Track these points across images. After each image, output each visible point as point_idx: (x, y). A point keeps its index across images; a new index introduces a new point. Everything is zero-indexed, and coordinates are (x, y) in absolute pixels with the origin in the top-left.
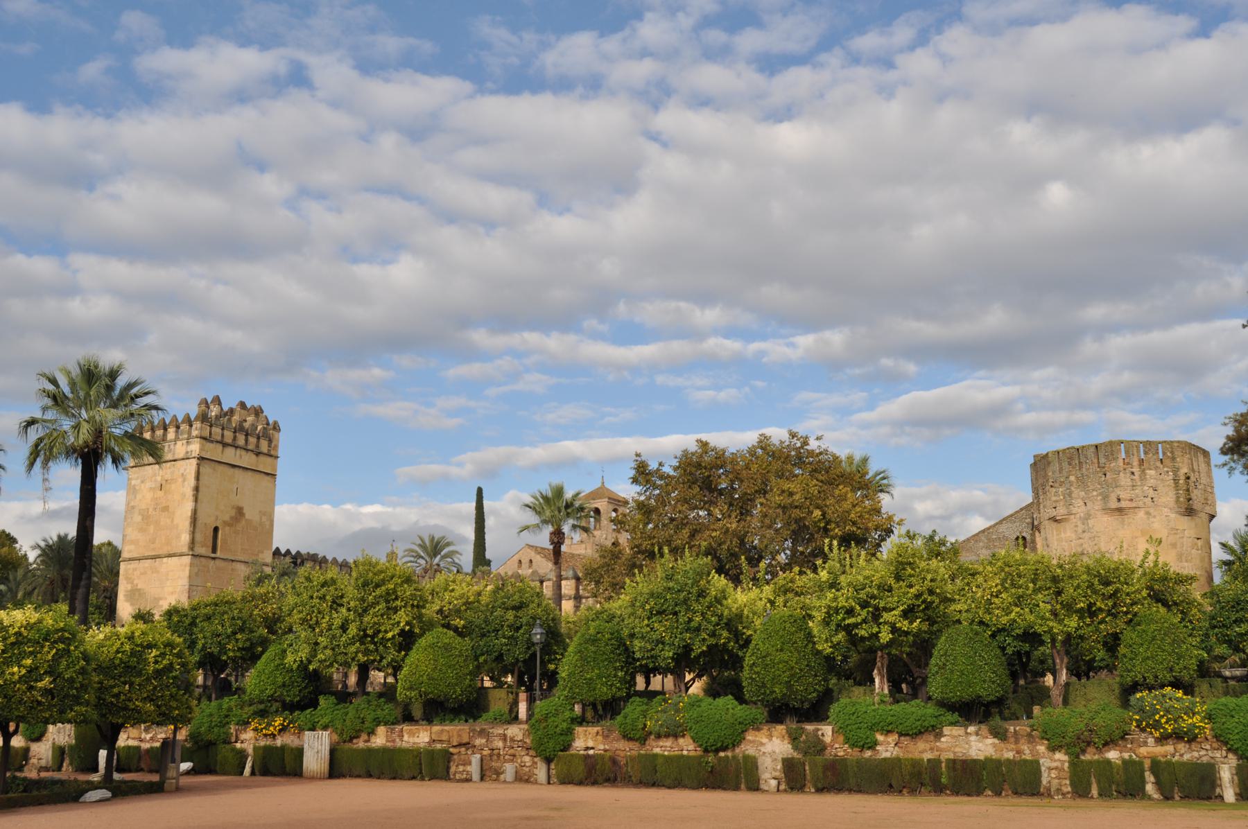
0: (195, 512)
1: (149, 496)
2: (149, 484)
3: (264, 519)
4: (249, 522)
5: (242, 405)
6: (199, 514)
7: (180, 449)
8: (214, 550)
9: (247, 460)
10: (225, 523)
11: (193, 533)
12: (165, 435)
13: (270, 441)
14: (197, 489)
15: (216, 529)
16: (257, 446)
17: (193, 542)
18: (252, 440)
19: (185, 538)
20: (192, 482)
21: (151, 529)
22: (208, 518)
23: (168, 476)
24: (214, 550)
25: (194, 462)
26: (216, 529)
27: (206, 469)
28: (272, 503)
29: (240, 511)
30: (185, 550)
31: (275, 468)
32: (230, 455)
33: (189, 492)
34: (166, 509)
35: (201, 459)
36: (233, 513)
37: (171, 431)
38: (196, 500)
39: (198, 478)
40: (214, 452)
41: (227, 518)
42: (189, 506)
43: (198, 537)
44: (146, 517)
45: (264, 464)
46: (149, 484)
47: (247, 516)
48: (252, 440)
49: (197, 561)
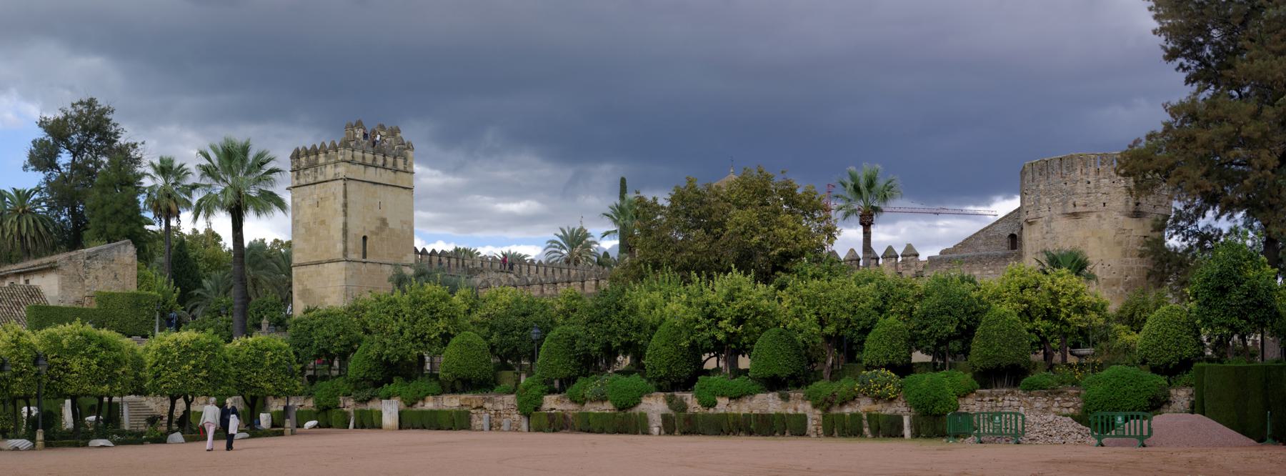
0: (345, 224)
1: (309, 211)
2: (308, 202)
3: (405, 227)
4: (392, 230)
5: (382, 127)
6: (349, 226)
7: (330, 172)
8: (365, 256)
9: (387, 177)
10: (372, 233)
11: (345, 242)
12: (317, 159)
13: (406, 160)
14: (345, 205)
15: (365, 238)
16: (395, 164)
17: (346, 250)
18: (390, 160)
19: (340, 247)
20: (341, 199)
21: (314, 239)
22: (356, 229)
23: (322, 195)
24: (364, 257)
25: (341, 182)
26: (365, 238)
27: (352, 186)
28: (411, 213)
29: (384, 222)
30: (341, 257)
31: (411, 182)
32: (372, 174)
33: (340, 208)
34: (323, 222)
35: (346, 179)
36: (378, 223)
37: (322, 155)
38: (346, 214)
39: (345, 196)
40: (357, 171)
41: (373, 228)
42: (341, 219)
43: (350, 245)
44: (308, 230)
45: (401, 179)
46: (308, 202)
47: (391, 225)
48: (390, 160)
49: (350, 265)
